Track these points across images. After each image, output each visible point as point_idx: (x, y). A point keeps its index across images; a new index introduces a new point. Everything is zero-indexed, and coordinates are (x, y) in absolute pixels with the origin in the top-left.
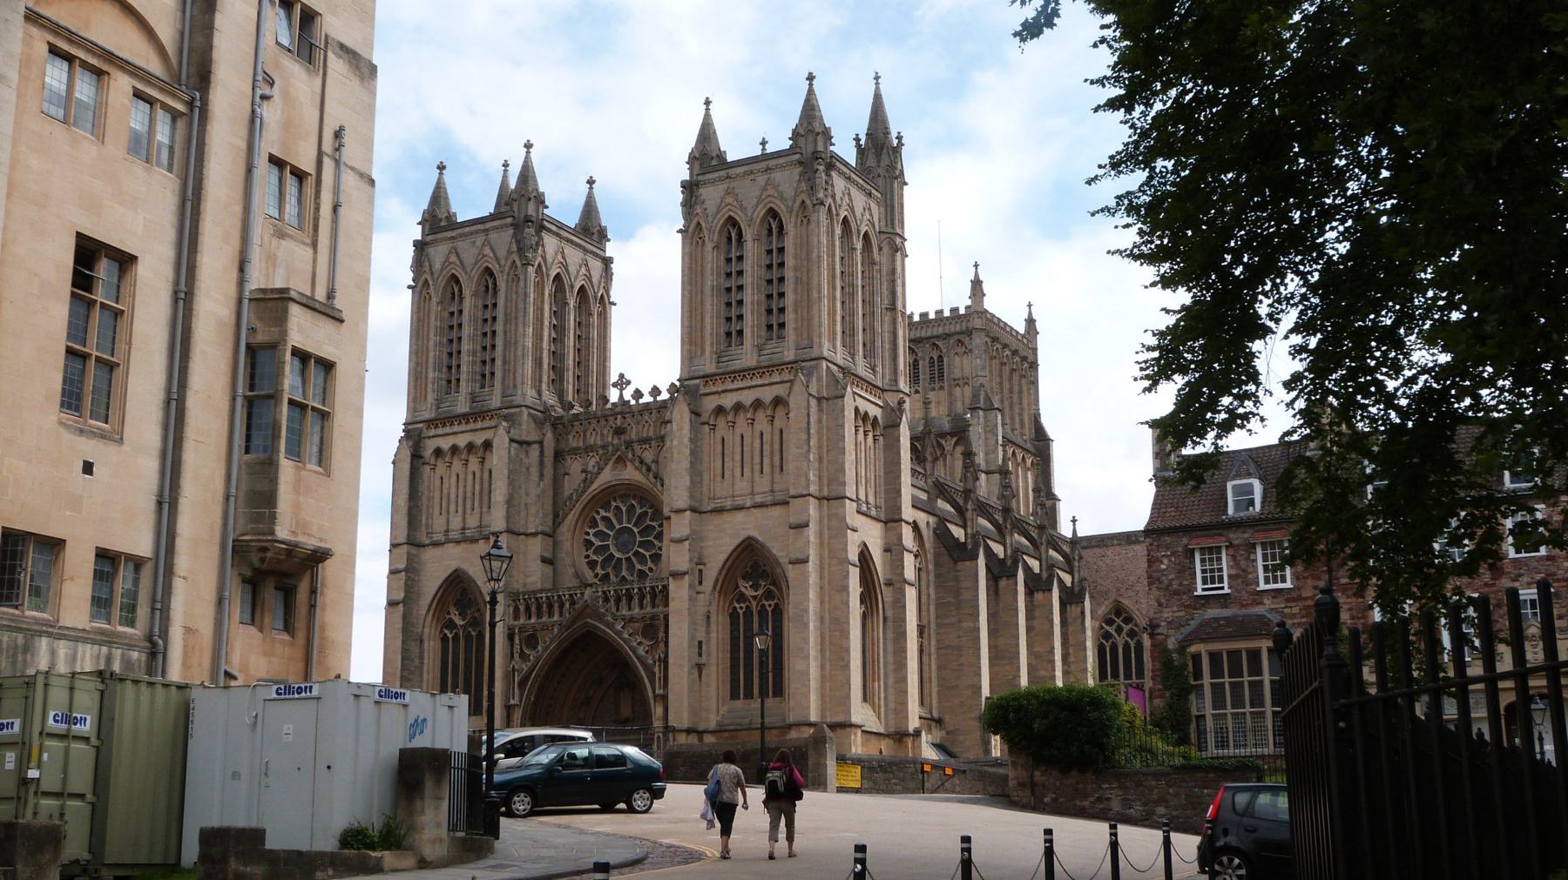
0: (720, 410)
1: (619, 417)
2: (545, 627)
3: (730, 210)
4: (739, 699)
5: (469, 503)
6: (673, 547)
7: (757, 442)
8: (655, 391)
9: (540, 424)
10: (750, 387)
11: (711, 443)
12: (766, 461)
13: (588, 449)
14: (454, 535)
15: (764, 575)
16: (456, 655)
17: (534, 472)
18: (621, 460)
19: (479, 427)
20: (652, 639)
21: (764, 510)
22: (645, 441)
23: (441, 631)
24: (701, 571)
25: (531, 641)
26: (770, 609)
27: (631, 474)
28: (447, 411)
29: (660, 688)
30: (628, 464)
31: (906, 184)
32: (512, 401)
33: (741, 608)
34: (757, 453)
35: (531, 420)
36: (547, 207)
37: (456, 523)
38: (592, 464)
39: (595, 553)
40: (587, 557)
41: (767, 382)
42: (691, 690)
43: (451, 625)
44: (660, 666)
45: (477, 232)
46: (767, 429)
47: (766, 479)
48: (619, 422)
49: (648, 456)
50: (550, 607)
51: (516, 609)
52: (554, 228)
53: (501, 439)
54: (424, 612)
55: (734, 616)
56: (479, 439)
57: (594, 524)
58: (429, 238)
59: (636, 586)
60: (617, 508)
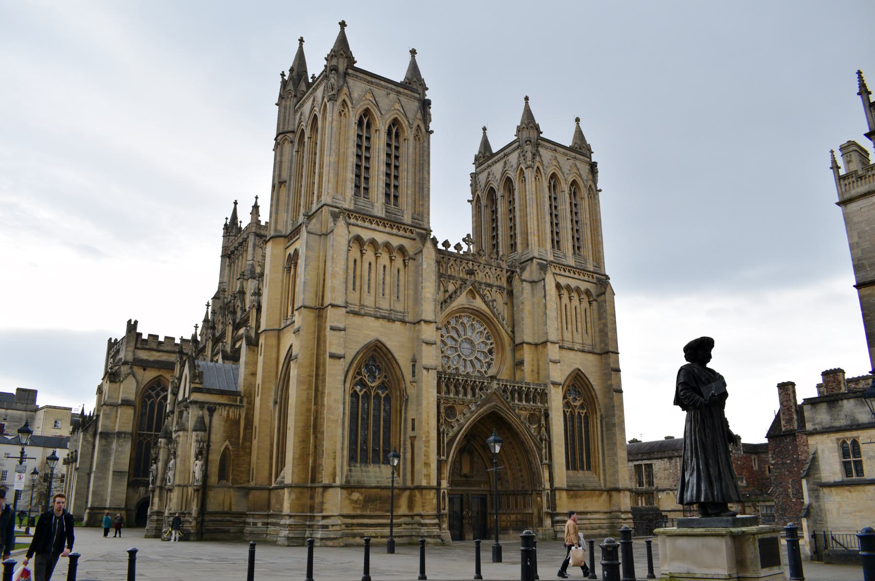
1: (471, 263)
6: (551, 365)
12: (579, 324)
13: (451, 277)
19: (394, 233)
21: (583, 354)
23: (353, 388)
25: (451, 411)
26: (583, 415)
27: (479, 303)
29: (546, 459)
32: (420, 225)
38: (451, 288)
43: (362, 383)
44: (545, 444)
45: (391, 89)
48: (471, 266)
59: (532, 386)
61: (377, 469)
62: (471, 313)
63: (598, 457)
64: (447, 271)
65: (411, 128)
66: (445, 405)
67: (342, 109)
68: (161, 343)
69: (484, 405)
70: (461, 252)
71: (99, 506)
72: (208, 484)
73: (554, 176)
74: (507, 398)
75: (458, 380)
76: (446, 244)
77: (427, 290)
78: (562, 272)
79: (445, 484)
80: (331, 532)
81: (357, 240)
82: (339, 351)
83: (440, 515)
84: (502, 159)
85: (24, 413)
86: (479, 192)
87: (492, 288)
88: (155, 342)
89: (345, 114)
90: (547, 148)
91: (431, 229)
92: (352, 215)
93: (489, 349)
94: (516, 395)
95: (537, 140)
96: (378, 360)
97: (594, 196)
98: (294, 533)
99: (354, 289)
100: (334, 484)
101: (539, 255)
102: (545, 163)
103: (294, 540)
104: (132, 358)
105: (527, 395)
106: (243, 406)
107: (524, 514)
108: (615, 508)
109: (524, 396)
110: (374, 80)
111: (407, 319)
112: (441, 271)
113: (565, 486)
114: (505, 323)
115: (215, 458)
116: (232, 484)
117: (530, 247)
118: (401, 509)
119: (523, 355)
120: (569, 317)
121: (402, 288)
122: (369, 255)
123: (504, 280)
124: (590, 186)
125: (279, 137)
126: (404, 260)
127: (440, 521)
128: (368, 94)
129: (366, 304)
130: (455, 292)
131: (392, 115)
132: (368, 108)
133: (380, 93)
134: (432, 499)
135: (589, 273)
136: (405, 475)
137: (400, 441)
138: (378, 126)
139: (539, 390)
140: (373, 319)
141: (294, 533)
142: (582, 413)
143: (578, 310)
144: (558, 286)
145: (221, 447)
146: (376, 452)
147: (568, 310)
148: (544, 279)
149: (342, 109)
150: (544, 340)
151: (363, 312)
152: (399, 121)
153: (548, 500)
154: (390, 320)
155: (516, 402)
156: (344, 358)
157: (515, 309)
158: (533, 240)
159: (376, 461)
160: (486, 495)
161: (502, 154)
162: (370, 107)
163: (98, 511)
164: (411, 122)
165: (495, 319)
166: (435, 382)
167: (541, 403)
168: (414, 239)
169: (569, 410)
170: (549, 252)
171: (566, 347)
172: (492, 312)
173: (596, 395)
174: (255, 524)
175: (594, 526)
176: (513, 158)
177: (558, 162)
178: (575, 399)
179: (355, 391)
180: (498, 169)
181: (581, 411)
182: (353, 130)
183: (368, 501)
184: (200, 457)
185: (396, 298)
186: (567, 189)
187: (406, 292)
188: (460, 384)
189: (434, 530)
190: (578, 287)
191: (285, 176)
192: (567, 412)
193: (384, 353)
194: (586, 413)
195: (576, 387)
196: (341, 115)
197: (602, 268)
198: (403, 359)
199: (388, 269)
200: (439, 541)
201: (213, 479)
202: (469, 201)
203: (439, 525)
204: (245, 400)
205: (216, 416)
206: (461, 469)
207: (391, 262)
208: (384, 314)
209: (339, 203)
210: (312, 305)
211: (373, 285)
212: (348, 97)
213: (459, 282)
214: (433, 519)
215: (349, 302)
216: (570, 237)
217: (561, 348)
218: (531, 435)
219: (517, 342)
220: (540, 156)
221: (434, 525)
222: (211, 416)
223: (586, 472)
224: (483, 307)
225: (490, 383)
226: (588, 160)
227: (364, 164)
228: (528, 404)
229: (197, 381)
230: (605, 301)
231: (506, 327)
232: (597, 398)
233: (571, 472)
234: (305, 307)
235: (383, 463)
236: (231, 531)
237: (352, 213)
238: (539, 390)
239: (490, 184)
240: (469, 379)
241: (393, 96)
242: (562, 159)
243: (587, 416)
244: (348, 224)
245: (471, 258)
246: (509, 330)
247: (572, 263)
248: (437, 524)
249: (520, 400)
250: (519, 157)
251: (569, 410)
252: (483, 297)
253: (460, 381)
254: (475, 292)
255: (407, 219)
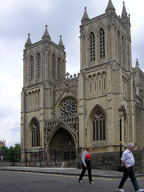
0: (90, 76)
2: (52, 128)
5: (36, 103)
7: (99, 83)
8: (75, 75)
9: (50, 85)
10: (97, 70)
11: (88, 85)
13: (61, 90)
14: (33, 110)
15: (101, 113)
17: (49, 96)
18: (68, 91)
20: (75, 129)
22: (72, 86)
24: (86, 113)
25: (49, 130)
27: (70, 94)
30: (69, 92)
31: (131, 26)
33: (95, 121)
34: (99, 85)
35: (48, 84)
36: (51, 39)
37: (34, 107)
39: (63, 112)
40: (61, 113)
42: (84, 139)
46: (101, 79)
47: (101, 91)
49: (74, 90)
50: (53, 123)
51: (46, 124)
52: (52, 43)
53: (42, 89)
55: (94, 123)
56: (37, 89)
57: (62, 105)
58: (26, 49)
60: (67, 102)
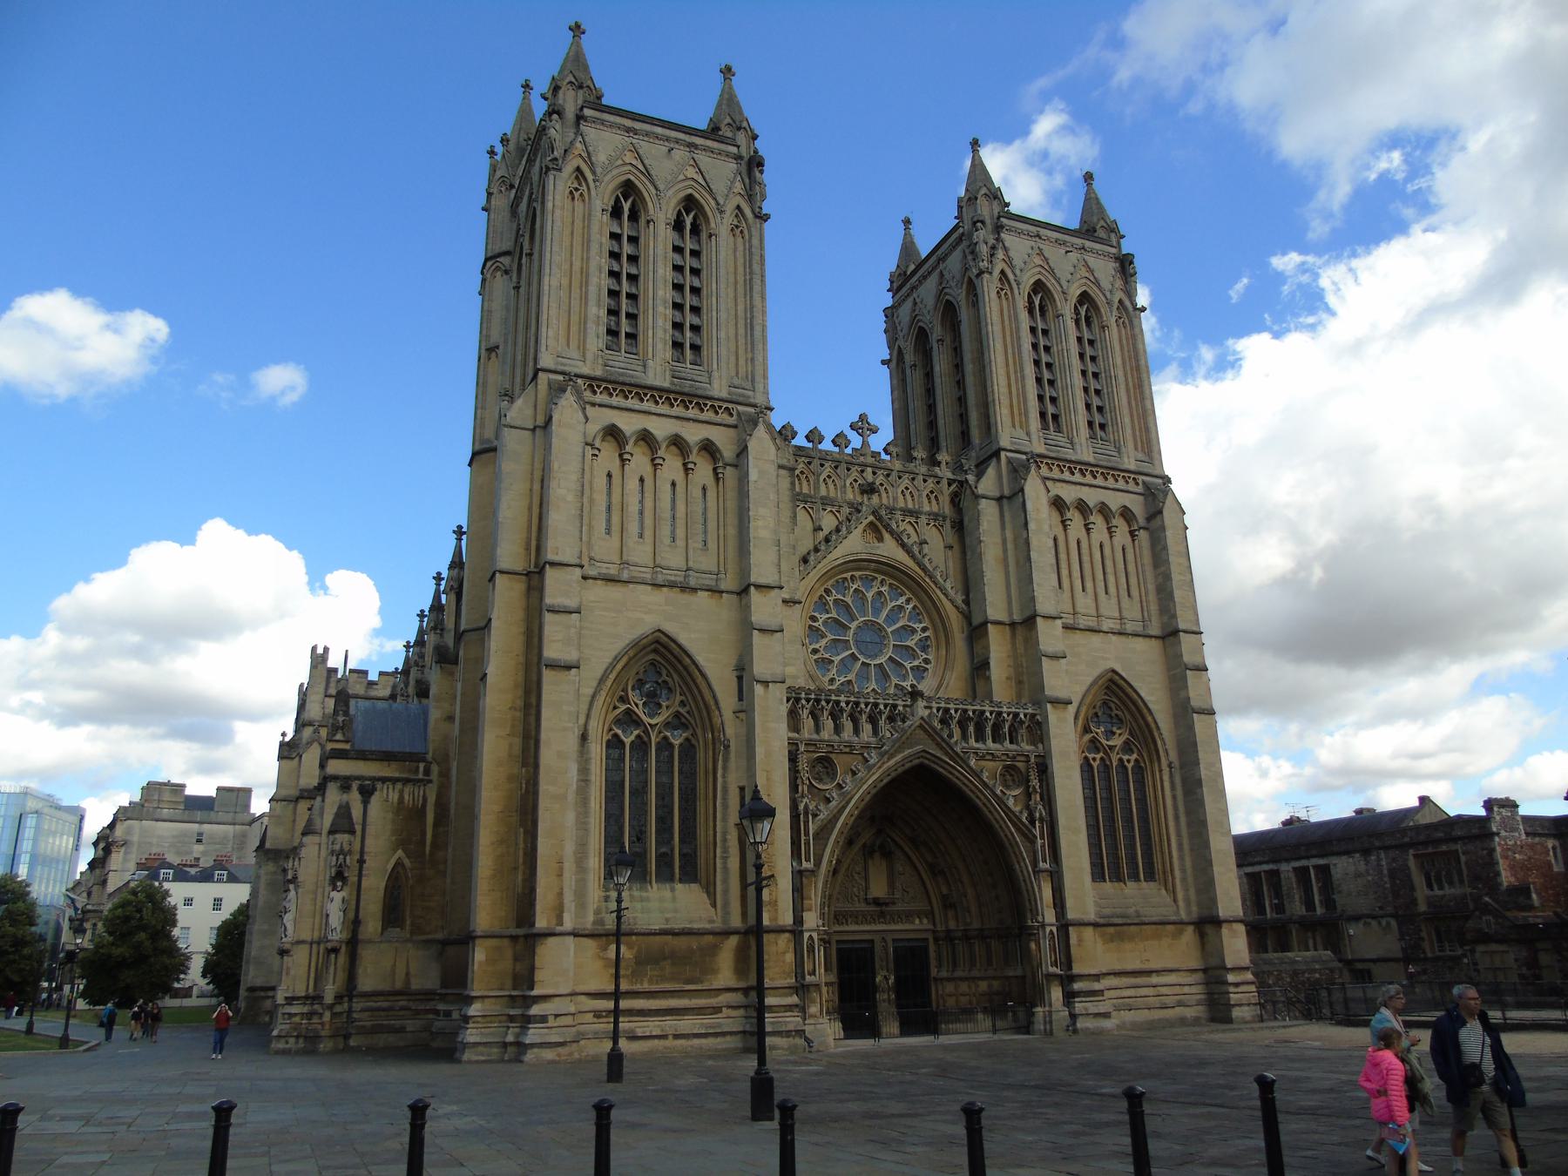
3: (1040, 273)
4: (1105, 881)
12: (1111, 579)
16: (641, 773)
19: (691, 416)
21: (1123, 638)
23: (611, 730)
25: (825, 765)
26: (1130, 766)
27: (889, 549)
28: (622, 374)
38: (828, 522)
41: (1111, 486)
43: (629, 719)
54: (590, 691)
61: (667, 894)
62: (875, 571)
63: (1170, 853)
64: (817, 488)
65: (721, 212)
66: (810, 755)
67: (576, 185)
68: (371, 683)
69: (897, 752)
70: (848, 451)
71: (264, 985)
72: (360, 937)
73: (1038, 286)
74: (951, 736)
75: (838, 703)
76: (814, 436)
77: (760, 523)
78: (1067, 476)
79: (811, 920)
80: (554, 1030)
81: (611, 435)
82: (570, 655)
83: (803, 986)
84: (934, 268)
85: (230, 828)
86: (901, 342)
87: (917, 518)
88: (361, 683)
89: (581, 195)
90: (1020, 233)
91: (772, 404)
92: (599, 387)
93: (920, 640)
94: (971, 729)
95: (998, 218)
96: (664, 672)
97: (1131, 322)
98: (482, 1034)
99: (608, 531)
100: (559, 929)
101: (1012, 443)
102: (1018, 262)
103: (481, 1049)
104: (321, 714)
105: (997, 728)
106: (430, 781)
107: (1007, 978)
108: (1213, 962)
109: (989, 730)
110: (638, 126)
111: (723, 587)
112: (797, 489)
113: (1092, 917)
114: (948, 585)
115: (375, 884)
116: (412, 933)
117: (993, 430)
118: (720, 976)
119: (987, 648)
120: (1087, 566)
121: (712, 525)
122: (639, 460)
123: (945, 499)
124: (1120, 301)
125: (489, 264)
126: (715, 469)
127: (802, 999)
128: (628, 154)
129: (633, 559)
130: (838, 530)
131: (680, 190)
132: (629, 180)
133: (653, 152)
134: (784, 953)
135: (1126, 475)
136: (726, 904)
137: (715, 832)
138: (651, 212)
139: (1022, 716)
140: (649, 588)
141: (482, 1034)
142: (1129, 761)
143: (1107, 551)
144: (1058, 504)
145: (388, 860)
146: (664, 860)
147: (1085, 551)
148: (1022, 490)
149: (576, 185)
150: (1028, 613)
151: (625, 576)
152: (697, 200)
153: (1053, 949)
154: (685, 588)
155: (972, 741)
156: (578, 668)
157: (968, 557)
158: (1002, 415)
159: (665, 875)
160: (927, 939)
161: (934, 258)
162: (632, 178)
163: (262, 994)
164: (721, 202)
165: (927, 580)
166: (784, 708)
167: (1033, 743)
168: (735, 427)
169: (1098, 756)
170: (1034, 437)
171: (1081, 626)
172: (919, 564)
173: (1156, 723)
174: (448, 1014)
175: (1169, 1001)
176: (954, 263)
177: (1046, 259)
178: (1110, 734)
179: (616, 735)
180: (928, 291)
181: (1125, 758)
182: (602, 224)
183: (642, 961)
184: (339, 884)
185: (700, 545)
186: (1067, 310)
187: (721, 532)
188: (842, 710)
189: (788, 1019)
190: (1103, 503)
191: (496, 337)
192: (1094, 759)
193: (675, 657)
194: (1136, 760)
195: (1110, 708)
196: (573, 199)
197: (1156, 462)
198: (715, 665)
199: (680, 489)
200: (800, 1041)
201: (372, 926)
202: (883, 362)
203: (802, 1009)
204: (435, 769)
205: (375, 800)
206: (867, 888)
207: (687, 475)
208: (673, 578)
209: (570, 365)
210: (519, 567)
211: (648, 521)
212: (585, 161)
213: (846, 510)
214: (791, 995)
215: (597, 558)
216: (1081, 406)
217: (1066, 627)
218: (1007, 810)
219: (976, 621)
220: (1006, 249)
221: (790, 1008)
222: (366, 803)
223: (1144, 884)
224: (901, 556)
225: (910, 706)
226: (1113, 250)
227: (626, 287)
228: (998, 746)
229: (339, 736)
230: (1163, 528)
231: (952, 593)
232: (1158, 728)
233: (1108, 887)
234: (502, 572)
235: (681, 881)
236: (408, 1029)
237: (598, 383)
238: (1022, 716)
239: (919, 321)
240: (862, 700)
241: (680, 154)
242: (1054, 254)
243: (1141, 767)
244: (584, 405)
245: (870, 460)
246: (959, 599)
247: (1092, 460)
248: (797, 1006)
249: (980, 737)
250: (965, 257)
251: (1098, 756)
252: (898, 537)
253: (843, 705)
254: (881, 527)
255: (719, 389)
